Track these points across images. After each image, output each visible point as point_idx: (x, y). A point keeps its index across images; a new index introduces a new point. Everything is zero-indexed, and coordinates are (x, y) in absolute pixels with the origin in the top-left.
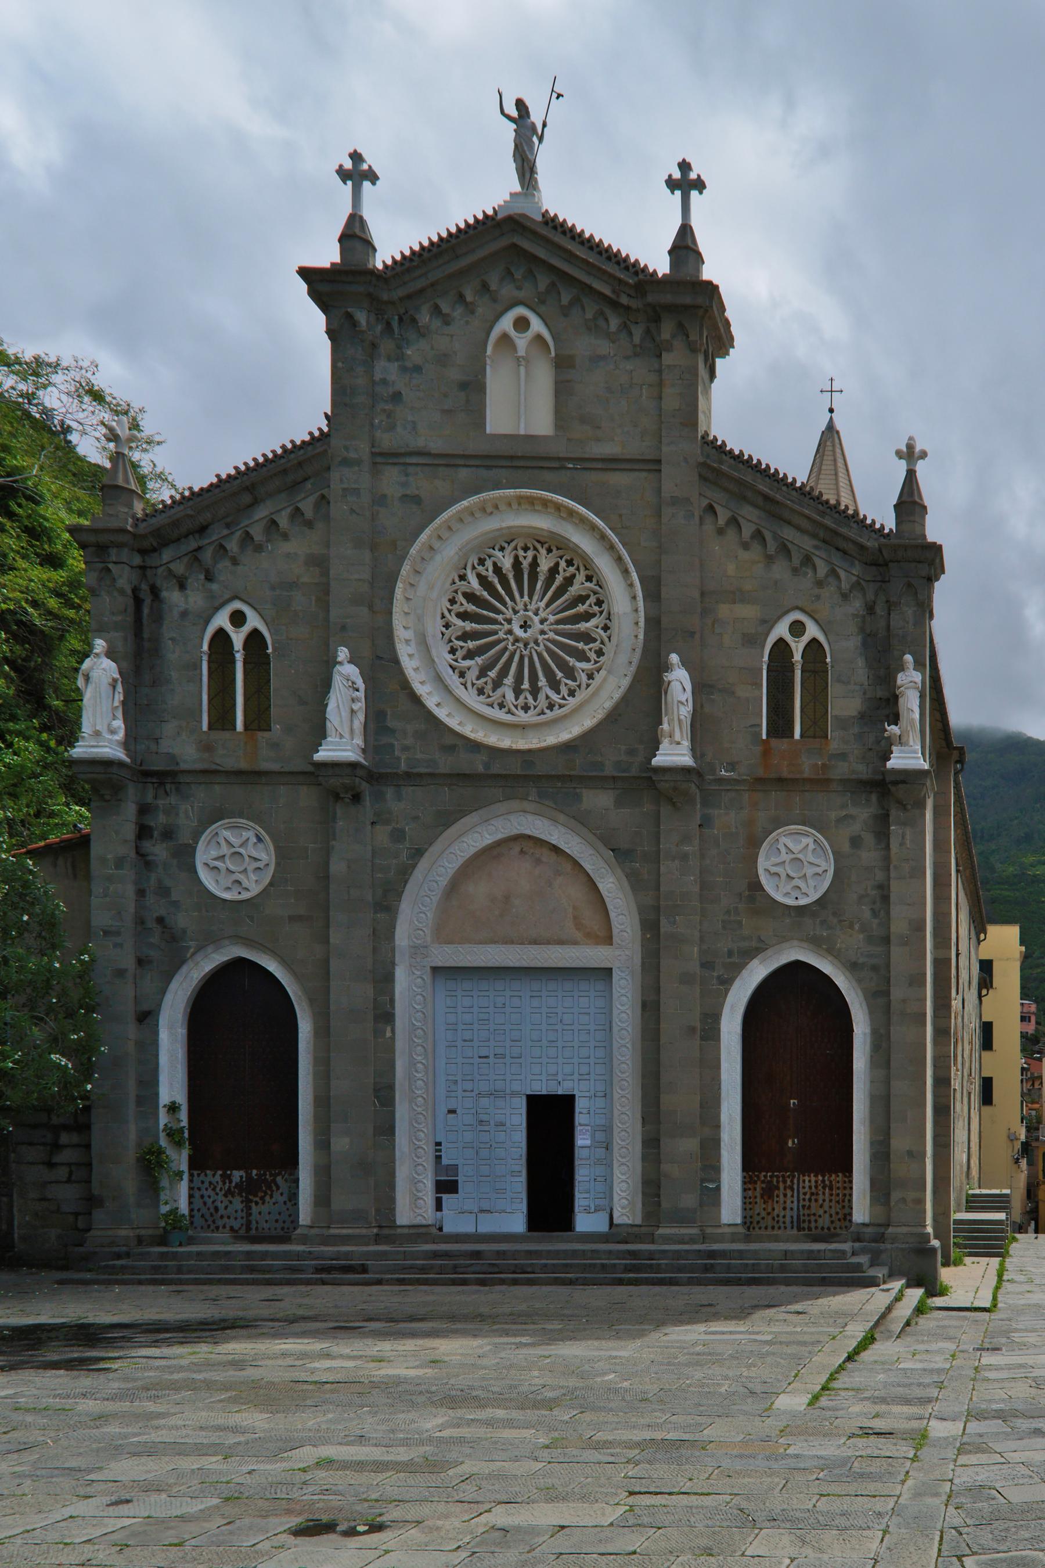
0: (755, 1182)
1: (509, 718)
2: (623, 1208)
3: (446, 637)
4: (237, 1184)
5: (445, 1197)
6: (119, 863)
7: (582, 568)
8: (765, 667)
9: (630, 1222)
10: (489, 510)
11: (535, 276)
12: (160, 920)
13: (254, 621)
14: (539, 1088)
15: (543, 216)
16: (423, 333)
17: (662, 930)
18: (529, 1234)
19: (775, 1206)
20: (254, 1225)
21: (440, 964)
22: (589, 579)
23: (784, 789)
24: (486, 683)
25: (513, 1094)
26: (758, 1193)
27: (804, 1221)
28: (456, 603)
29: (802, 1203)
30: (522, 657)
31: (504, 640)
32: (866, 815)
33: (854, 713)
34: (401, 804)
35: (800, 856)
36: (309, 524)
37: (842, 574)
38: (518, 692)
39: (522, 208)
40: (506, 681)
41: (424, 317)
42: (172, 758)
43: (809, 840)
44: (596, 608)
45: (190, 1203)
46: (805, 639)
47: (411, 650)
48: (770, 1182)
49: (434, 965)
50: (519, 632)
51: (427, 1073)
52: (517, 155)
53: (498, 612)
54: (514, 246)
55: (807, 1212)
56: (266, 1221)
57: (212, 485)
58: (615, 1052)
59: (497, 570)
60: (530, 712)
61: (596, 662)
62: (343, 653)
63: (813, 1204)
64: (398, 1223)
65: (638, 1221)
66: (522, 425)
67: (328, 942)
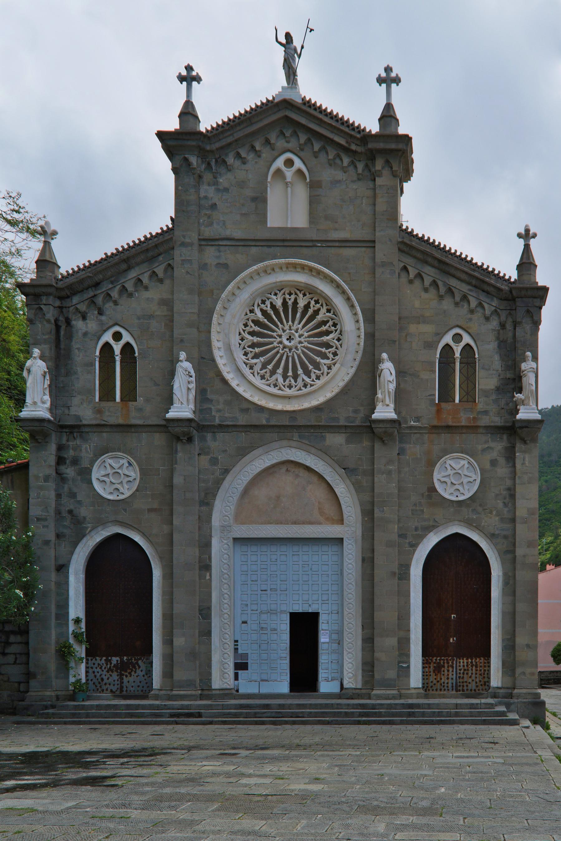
0: (430, 663)
1: (280, 392)
2: (349, 678)
3: (242, 346)
4: (114, 665)
5: (240, 672)
6: (46, 479)
7: (324, 305)
8: (437, 361)
9: (354, 687)
10: (268, 272)
11: (298, 136)
12: (70, 512)
13: (127, 337)
14: (297, 608)
15: (303, 100)
16: (229, 169)
17: (375, 515)
18: (292, 694)
19: (442, 677)
20: (125, 689)
21: (238, 536)
22: (329, 311)
23: (449, 432)
24: (266, 372)
25: (282, 612)
26: (432, 669)
27: (460, 686)
28: (248, 326)
29: (458, 675)
30: (288, 357)
31: (277, 347)
32: (500, 447)
33: (493, 387)
34: (216, 443)
35: (460, 472)
36: (161, 281)
37: (486, 305)
38: (285, 377)
39: (289, 95)
40: (278, 371)
41: (230, 159)
42: (78, 418)
43: (465, 462)
44: (333, 328)
45: (87, 676)
46: (462, 344)
47: (221, 353)
48: (440, 663)
49: (234, 537)
50: (287, 343)
51: (230, 600)
52: (286, 65)
53: (273, 331)
54: (286, 117)
55: (461, 680)
56: (132, 687)
57: (102, 259)
58: (345, 587)
59: (273, 307)
60: (293, 389)
61: (333, 360)
62: (183, 355)
63: (465, 676)
64: (213, 688)
65: (359, 686)
66: (289, 222)
67: (172, 524)
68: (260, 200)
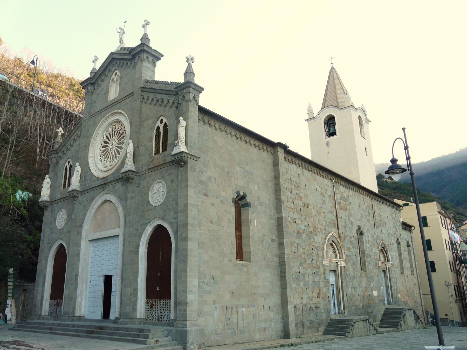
13: (71, 163)
68: (107, 93)
